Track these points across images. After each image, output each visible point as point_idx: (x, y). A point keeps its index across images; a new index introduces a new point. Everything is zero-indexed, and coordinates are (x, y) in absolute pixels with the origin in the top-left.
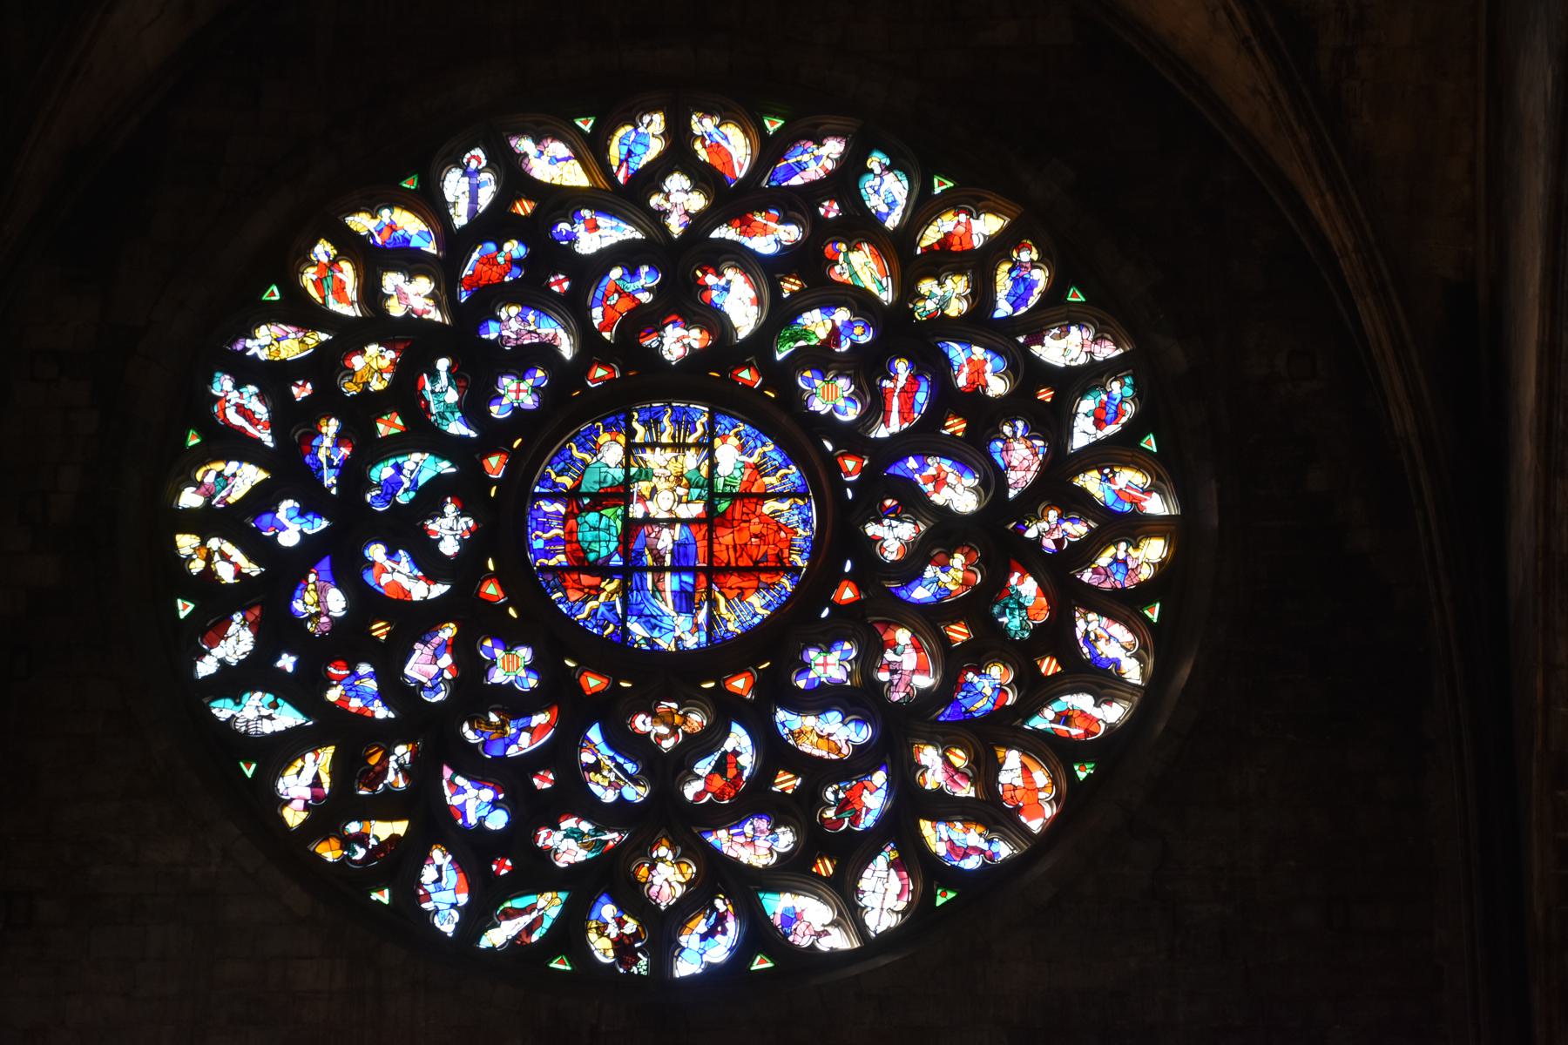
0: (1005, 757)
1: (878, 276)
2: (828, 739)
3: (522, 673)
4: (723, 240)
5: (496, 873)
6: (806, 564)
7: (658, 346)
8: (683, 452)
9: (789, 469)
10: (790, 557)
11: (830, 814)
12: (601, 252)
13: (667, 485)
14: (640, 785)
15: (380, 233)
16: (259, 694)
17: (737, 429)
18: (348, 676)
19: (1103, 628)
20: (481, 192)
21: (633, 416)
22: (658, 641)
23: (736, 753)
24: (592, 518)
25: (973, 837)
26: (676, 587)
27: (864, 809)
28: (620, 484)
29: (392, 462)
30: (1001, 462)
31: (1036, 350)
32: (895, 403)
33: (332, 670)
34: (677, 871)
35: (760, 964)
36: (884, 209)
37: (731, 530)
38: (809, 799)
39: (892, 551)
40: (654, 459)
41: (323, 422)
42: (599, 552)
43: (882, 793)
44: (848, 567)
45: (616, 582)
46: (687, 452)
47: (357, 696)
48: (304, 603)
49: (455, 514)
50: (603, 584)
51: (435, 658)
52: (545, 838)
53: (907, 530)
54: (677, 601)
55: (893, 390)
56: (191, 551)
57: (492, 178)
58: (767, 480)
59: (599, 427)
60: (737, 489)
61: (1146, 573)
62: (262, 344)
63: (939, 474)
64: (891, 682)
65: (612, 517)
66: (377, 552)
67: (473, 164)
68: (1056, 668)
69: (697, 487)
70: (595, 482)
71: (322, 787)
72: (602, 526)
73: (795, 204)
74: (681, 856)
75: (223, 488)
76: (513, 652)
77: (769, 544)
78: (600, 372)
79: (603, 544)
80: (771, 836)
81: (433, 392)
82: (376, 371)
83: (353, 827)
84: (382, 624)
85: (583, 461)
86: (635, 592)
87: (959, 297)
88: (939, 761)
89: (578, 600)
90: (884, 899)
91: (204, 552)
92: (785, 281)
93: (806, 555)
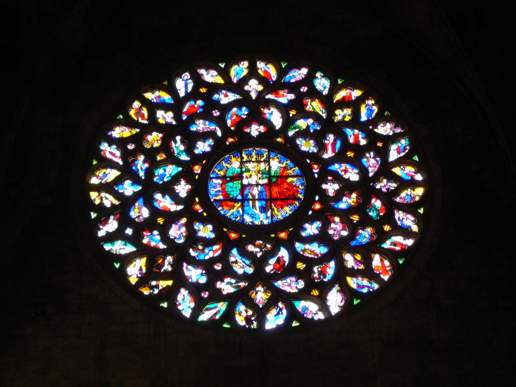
0: (374, 256)
1: (322, 109)
2: (314, 252)
3: (210, 233)
4: (269, 99)
5: (203, 297)
6: (303, 197)
7: (250, 131)
8: (260, 163)
9: (295, 168)
10: (297, 195)
11: (316, 275)
12: (229, 103)
13: (255, 174)
14: (251, 267)
15: (156, 98)
16: (120, 241)
17: (277, 156)
18: (151, 235)
19: (404, 216)
20: (188, 86)
21: (243, 153)
22: (255, 222)
23: (283, 257)
24: (231, 184)
25: (365, 282)
26: (260, 205)
27: (327, 274)
28: (239, 174)
29: (162, 168)
30: (366, 166)
31: (376, 130)
32: (330, 148)
33: (145, 233)
34: (265, 294)
35: (295, 324)
36: (322, 89)
37: (277, 187)
38: (309, 271)
39: (331, 193)
40: (250, 166)
41: (138, 156)
42: (233, 195)
43: (333, 269)
44: (317, 198)
45: (240, 204)
46: (261, 163)
47: (154, 241)
48: (134, 212)
49: (185, 184)
50: (235, 205)
51: (179, 229)
52: (219, 285)
53: (336, 186)
54: (260, 209)
55: (329, 143)
56: (95, 197)
57: (192, 81)
58: (288, 172)
59: (231, 157)
60: (279, 174)
61: (417, 199)
62: (118, 133)
63: (346, 169)
64: (334, 234)
65: (237, 184)
66: (158, 196)
67: (186, 78)
68: (389, 228)
69: (265, 174)
70: (231, 173)
71: (142, 270)
72: (234, 186)
73: (293, 87)
74: (266, 289)
75: (106, 177)
76: (206, 226)
77: (290, 191)
78: (231, 140)
79: (235, 192)
80: (296, 283)
81: (175, 147)
82: (156, 140)
83: (154, 283)
84: (161, 219)
85: (227, 167)
86: (246, 207)
87: (349, 115)
88: (352, 258)
89: (227, 210)
90: (336, 302)
91: (100, 197)
92: (291, 111)
93: (303, 194)
